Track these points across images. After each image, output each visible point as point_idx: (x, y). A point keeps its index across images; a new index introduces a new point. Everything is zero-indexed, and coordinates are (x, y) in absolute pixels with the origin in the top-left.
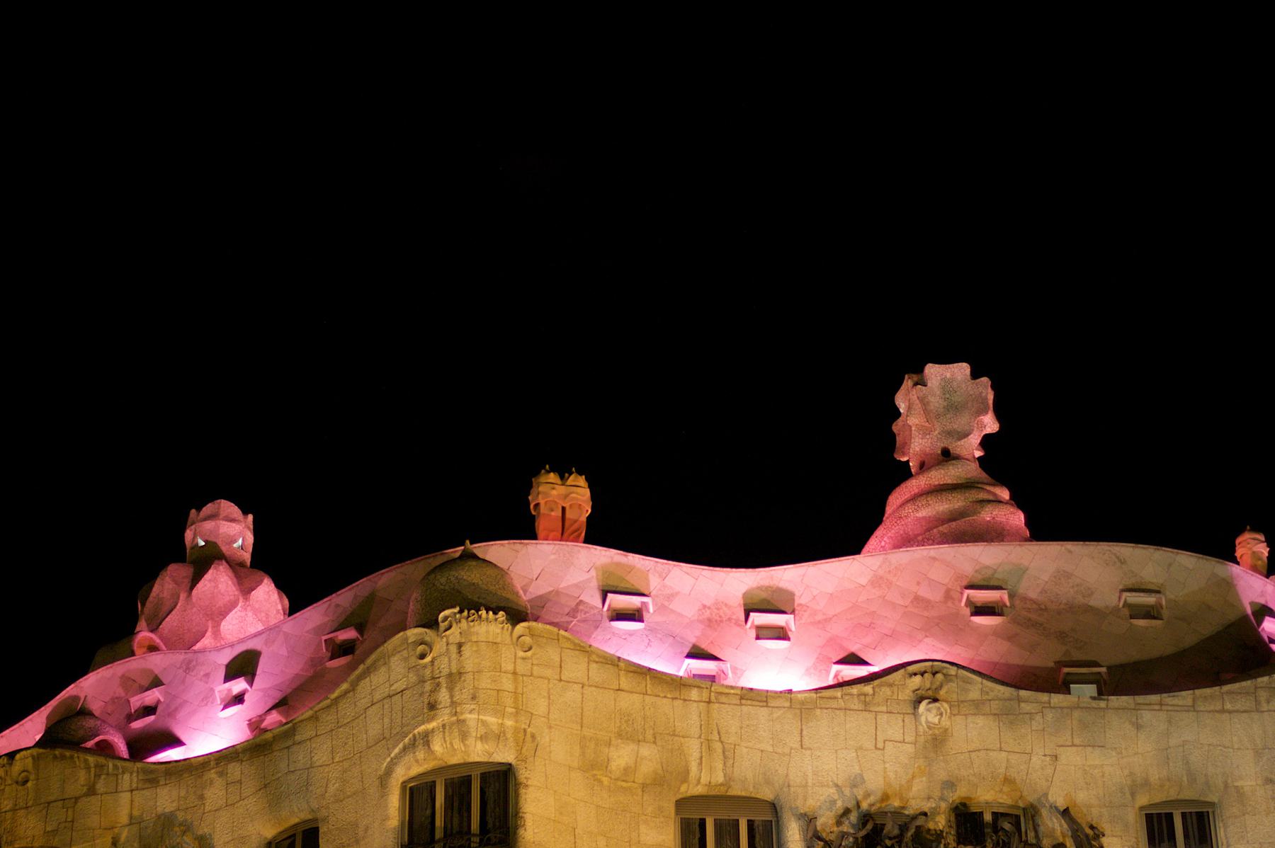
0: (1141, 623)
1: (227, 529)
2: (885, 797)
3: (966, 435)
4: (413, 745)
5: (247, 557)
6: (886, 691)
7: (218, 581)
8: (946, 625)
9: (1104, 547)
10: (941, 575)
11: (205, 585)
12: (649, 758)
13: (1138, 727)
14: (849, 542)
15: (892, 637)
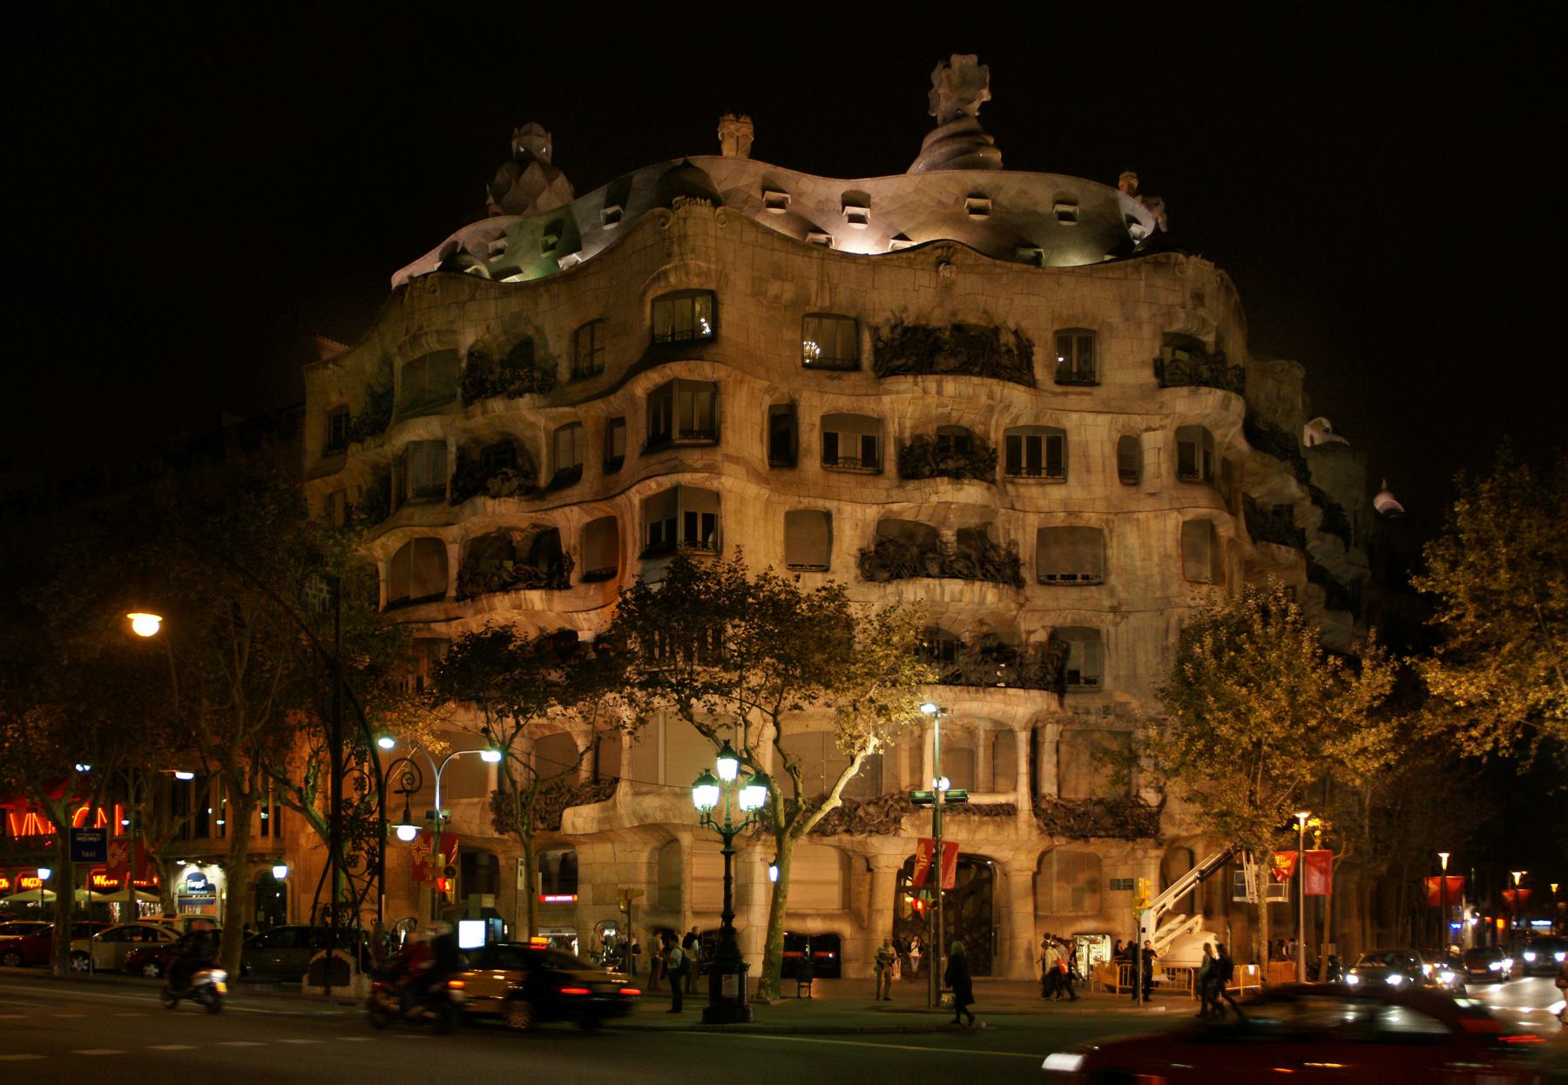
0: (1065, 223)
1: (537, 141)
2: (918, 318)
3: (971, 101)
4: (657, 279)
5: (548, 159)
6: (922, 257)
7: (533, 174)
8: (955, 220)
9: (1048, 176)
10: (954, 189)
11: (527, 175)
12: (789, 291)
13: (1059, 285)
14: (900, 167)
15: (923, 226)
